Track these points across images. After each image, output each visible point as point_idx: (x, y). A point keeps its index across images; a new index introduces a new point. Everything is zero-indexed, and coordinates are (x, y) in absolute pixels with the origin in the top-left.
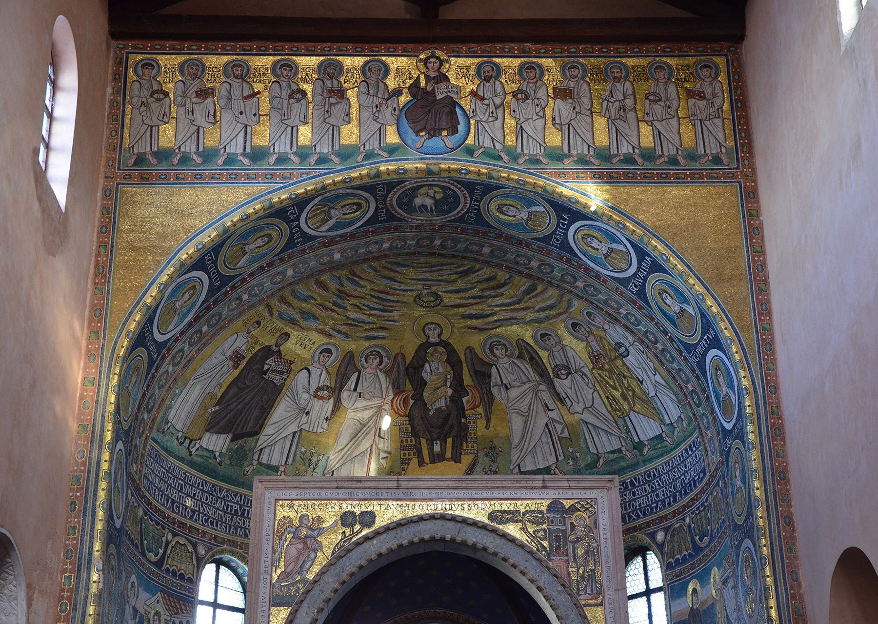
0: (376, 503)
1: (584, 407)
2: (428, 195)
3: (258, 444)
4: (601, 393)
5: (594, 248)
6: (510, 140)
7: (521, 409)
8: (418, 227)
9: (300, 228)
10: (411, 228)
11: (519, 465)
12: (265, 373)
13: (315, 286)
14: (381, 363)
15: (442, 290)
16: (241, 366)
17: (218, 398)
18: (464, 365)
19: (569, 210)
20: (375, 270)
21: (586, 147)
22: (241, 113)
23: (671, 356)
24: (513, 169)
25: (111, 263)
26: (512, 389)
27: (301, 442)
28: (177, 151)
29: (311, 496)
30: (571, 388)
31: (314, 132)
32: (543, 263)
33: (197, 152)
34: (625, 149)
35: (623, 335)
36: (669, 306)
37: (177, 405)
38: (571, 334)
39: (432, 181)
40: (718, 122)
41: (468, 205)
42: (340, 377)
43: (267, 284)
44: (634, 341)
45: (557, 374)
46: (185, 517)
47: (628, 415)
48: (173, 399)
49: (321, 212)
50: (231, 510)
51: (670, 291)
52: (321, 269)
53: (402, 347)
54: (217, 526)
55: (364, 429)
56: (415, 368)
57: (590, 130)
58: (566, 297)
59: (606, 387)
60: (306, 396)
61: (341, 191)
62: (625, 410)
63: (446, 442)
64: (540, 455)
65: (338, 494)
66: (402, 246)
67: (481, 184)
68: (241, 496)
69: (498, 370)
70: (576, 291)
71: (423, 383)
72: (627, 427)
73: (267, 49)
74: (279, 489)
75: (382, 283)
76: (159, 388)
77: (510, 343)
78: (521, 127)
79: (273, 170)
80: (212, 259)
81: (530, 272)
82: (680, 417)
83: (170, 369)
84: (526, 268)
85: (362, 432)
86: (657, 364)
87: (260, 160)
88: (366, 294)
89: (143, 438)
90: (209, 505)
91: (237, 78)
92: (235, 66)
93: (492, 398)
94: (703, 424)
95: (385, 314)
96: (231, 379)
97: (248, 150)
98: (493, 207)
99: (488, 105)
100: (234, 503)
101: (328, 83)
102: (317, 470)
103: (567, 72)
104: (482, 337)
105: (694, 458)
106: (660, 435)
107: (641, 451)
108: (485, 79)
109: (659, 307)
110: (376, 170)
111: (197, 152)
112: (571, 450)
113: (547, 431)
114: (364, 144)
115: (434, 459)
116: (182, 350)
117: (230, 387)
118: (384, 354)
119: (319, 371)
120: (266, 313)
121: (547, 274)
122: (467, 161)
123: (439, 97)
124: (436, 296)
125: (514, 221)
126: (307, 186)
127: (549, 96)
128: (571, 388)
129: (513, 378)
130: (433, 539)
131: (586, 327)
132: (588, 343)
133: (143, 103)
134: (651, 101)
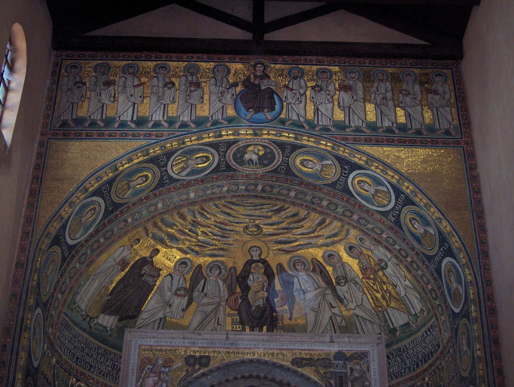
1: (355, 305)
3: (137, 325)
4: (368, 295)
5: (365, 190)
6: (310, 115)
8: (247, 176)
9: (167, 172)
13: (177, 217)
14: (220, 273)
16: (127, 270)
19: (349, 163)
20: (218, 207)
21: (360, 122)
22: (132, 96)
23: (417, 266)
24: (312, 134)
26: (308, 293)
28: (88, 118)
31: (179, 108)
33: (101, 120)
34: (387, 124)
35: (383, 254)
36: (416, 229)
37: (82, 292)
38: (348, 254)
39: (257, 141)
40: (447, 109)
41: (281, 160)
43: (144, 212)
44: (391, 257)
46: (85, 369)
47: (386, 310)
48: (79, 287)
50: (117, 368)
51: (418, 219)
54: (107, 377)
57: (363, 111)
58: (346, 227)
59: (371, 291)
60: (169, 293)
62: (384, 306)
63: (262, 328)
66: (236, 190)
67: (290, 144)
72: (385, 318)
73: (151, 57)
75: (222, 217)
76: (70, 278)
78: (317, 108)
82: (422, 309)
83: (78, 265)
84: (319, 207)
86: (407, 274)
87: (142, 125)
88: (211, 224)
89: (58, 311)
91: (130, 74)
92: (129, 67)
94: (438, 311)
96: (119, 278)
97: (135, 118)
98: (298, 162)
99: (295, 94)
101: (190, 78)
103: (348, 75)
104: (289, 256)
105: (432, 337)
106: (408, 323)
107: (394, 334)
108: (293, 78)
111: (101, 120)
113: (330, 321)
114: (212, 116)
116: (85, 254)
117: (118, 284)
118: (222, 267)
120: (143, 234)
122: (281, 128)
123: (263, 88)
124: (258, 227)
127: (336, 89)
128: (347, 292)
131: (358, 249)
132: (360, 260)
133: (69, 89)
134: (403, 94)
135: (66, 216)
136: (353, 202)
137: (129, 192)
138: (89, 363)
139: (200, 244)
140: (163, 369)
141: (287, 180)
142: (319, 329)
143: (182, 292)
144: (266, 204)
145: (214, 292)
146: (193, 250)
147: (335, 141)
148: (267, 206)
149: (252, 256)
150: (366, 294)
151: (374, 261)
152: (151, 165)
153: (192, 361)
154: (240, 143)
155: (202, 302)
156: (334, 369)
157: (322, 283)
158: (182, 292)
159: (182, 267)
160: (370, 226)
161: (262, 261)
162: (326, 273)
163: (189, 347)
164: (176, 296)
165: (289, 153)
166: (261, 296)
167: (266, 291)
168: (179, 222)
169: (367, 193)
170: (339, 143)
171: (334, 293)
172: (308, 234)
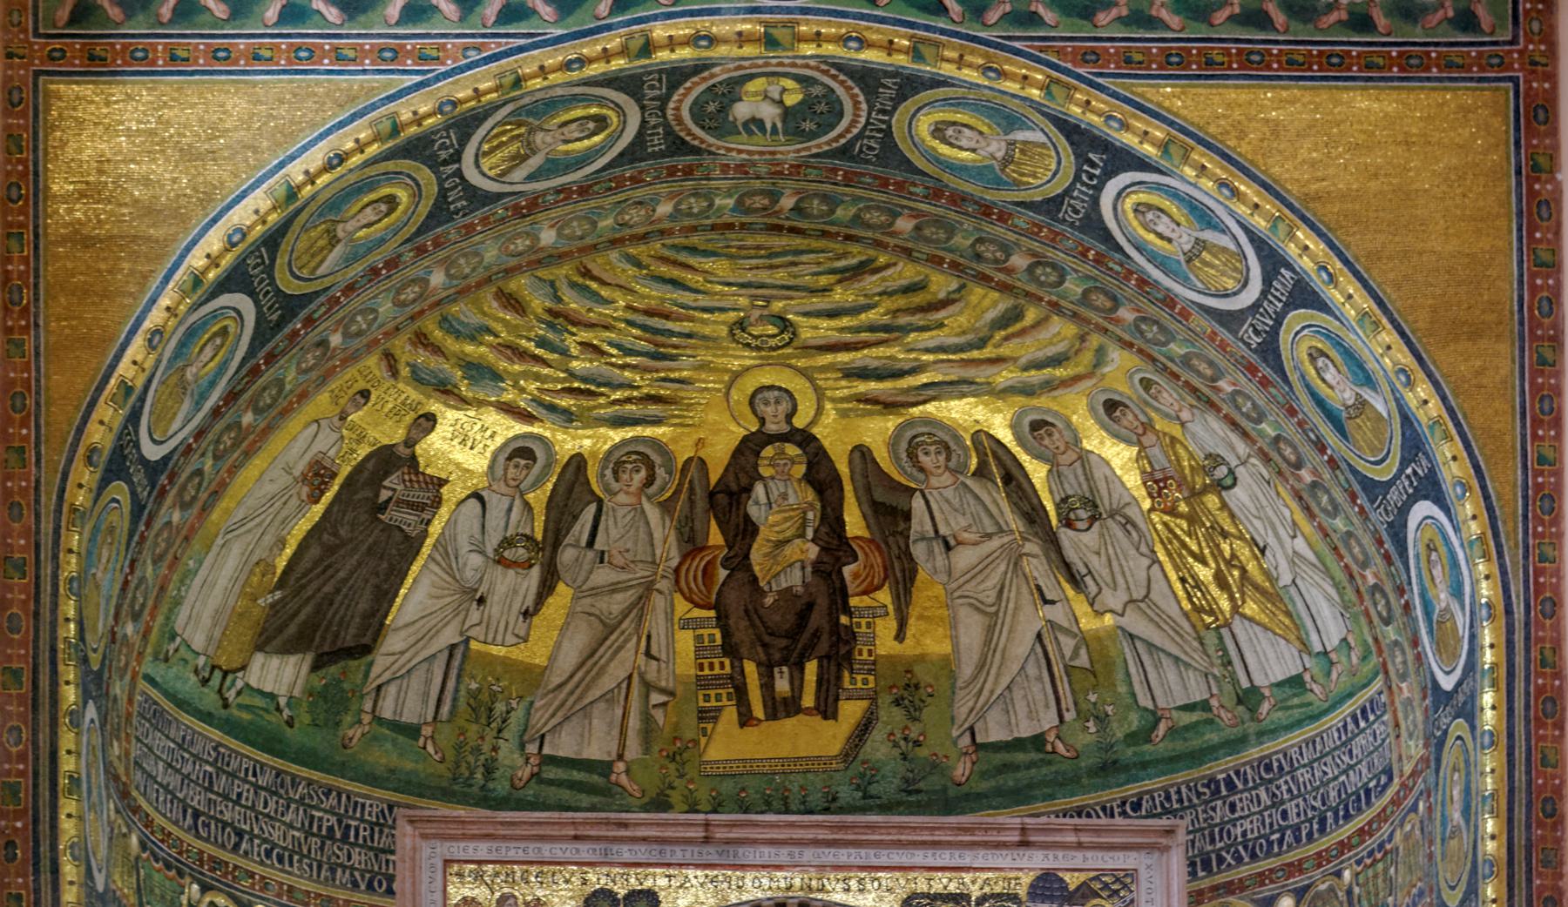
1: (1126, 598)
2: (766, 97)
4: (1169, 568)
7: (980, 596)
10: (725, 168)
11: (972, 730)
13: (495, 304)
14: (650, 480)
19: (1105, 146)
24: (974, 39)
26: (960, 548)
32: (1039, 261)
41: (863, 120)
53: (700, 442)
55: (613, 637)
56: (731, 494)
58: (1095, 340)
59: (1180, 555)
61: (559, 92)
63: (802, 670)
67: (895, 74)
69: (927, 502)
70: (1119, 332)
71: (749, 530)
77: (958, 438)
79: (396, 36)
81: (1009, 280)
84: (1000, 270)
98: (924, 125)
104: (891, 423)
110: (642, 41)
113: (1039, 649)
115: (774, 708)
119: (506, 502)
121: (1051, 285)
122: (863, 17)
126: (478, 81)
128: (1098, 553)
129: (963, 523)
131: (1137, 412)
132: (1142, 448)
136: (1117, 268)
142: (998, 675)
145: (629, 545)
146: (552, 408)
149: (762, 421)
150: (1160, 563)
151: (1192, 456)
154: (716, 70)
157: (1009, 515)
158: (521, 551)
159: (516, 466)
161: (798, 438)
162: (1025, 485)
165: (891, 99)
166: (795, 558)
167: (813, 541)
168: (503, 321)
171: (1053, 556)
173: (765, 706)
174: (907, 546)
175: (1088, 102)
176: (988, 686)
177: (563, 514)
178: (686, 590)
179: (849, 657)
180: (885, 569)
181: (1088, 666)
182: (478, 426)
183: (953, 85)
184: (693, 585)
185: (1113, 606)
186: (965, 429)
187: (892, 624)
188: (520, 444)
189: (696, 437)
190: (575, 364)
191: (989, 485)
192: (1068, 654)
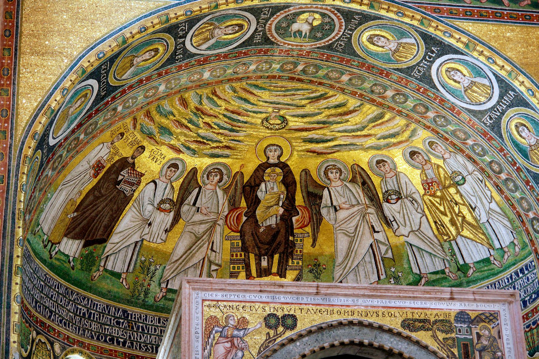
0: (297, 307)
1: (410, 230)
3: (105, 251)
4: (429, 217)
5: (455, 81)
7: (348, 230)
9: (184, 45)
12: (119, 183)
13: (178, 103)
14: (220, 180)
15: (290, 114)
16: (101, 175)
17: (77, 205)
18: (298, 186)
20: (235, 91)
25: (15, 65)
26: (341, 211)
27: (142, 251)
29: (236, 298)
30: (399, 213)
38: (408, 162)
41: (341, 33)
42: (182, 191)
43: (141, 98)
45: (387, 199)
46: (45, 317)
47: (454, 239)
49: (206, 31)
52: (189, 86)
53: (242, 166)
54: (69, 327)
55: (199, 242)
56: (251, 187)
58: (413, 126)
60: (150, 208)
61: (230, 12)
62: (452, 234)
64: (362, 273)
65: (261, 297)
68: (88, 300)
71: (257, 201)
72: (453, 250)
74: (206, 290)
75: (236, 104)
80: (107, 68)
81: (383, 101)
84: (380, 97)
85: (197, 244)
88: (219, 113)
90: (63, 307)
93: (320, 219)
95: (232, 134)
96: (90, 187)
100: (82, 306)
102: (154, 279)
104: (320, 160)
107: (465, 273)
109: (512, 139)
112: (393, 270)
113: (371, 251)
115: (261, 272)
116: (61, 156)
118: (225, 172)
119: (165, 185)
120: (131, 126)
121: (400, 103)
124: (284, 119)
125: (382, 51)
128: (399, 213)
129: (343, 200)
130: (352, 343)
132: (423, 170)
135: (57, 109)
136: (432, 95)
137: (129, 71)
138: (48, 308)
139: (199, 139)
140: (236, 332)
141: (342, 60)
142: (353, 261)
143: (167, 206)
144: (303, 90)
145: (209, 206)
146: (188, 148)
147: (425, 14)
148: (302, 91)
152: (166, 36)
153: (273, 321)
154: (291, 8)
155: (192, 220)
156: (456, 334)
158: (168, 205)
160: (450, 128)
161: (281, 165)
163: (267, 303)
164: (159, 211)
165: (356, 25)
167: (282, 206)
169: (457, 85)
170: (429, 15)
172: (353, 131)
173: (257, 272)
174: (320, 210)
175: (437, 26)
176: (348, 265)
177: (185, 191)
178: (229, 225)
179: (292, 253)
180: (310, 218)
181: (392, 257)
182: (159, 153)
183: (383, 19)
184: (232, 223)
185: (404, 234)
186: (349, 164)
187: (311, 240)
188: (173, 162)
189: (241, 163)
190: (200, 131)
191: (356, 185)
192: (383, 253)
